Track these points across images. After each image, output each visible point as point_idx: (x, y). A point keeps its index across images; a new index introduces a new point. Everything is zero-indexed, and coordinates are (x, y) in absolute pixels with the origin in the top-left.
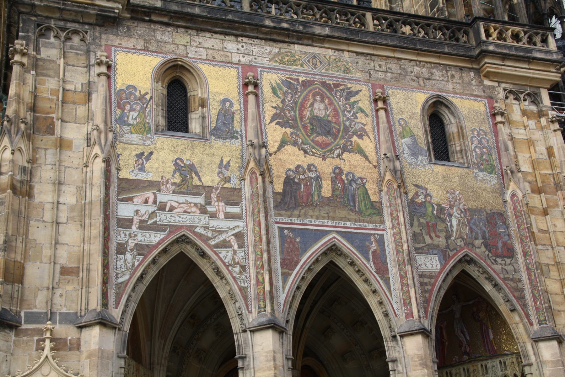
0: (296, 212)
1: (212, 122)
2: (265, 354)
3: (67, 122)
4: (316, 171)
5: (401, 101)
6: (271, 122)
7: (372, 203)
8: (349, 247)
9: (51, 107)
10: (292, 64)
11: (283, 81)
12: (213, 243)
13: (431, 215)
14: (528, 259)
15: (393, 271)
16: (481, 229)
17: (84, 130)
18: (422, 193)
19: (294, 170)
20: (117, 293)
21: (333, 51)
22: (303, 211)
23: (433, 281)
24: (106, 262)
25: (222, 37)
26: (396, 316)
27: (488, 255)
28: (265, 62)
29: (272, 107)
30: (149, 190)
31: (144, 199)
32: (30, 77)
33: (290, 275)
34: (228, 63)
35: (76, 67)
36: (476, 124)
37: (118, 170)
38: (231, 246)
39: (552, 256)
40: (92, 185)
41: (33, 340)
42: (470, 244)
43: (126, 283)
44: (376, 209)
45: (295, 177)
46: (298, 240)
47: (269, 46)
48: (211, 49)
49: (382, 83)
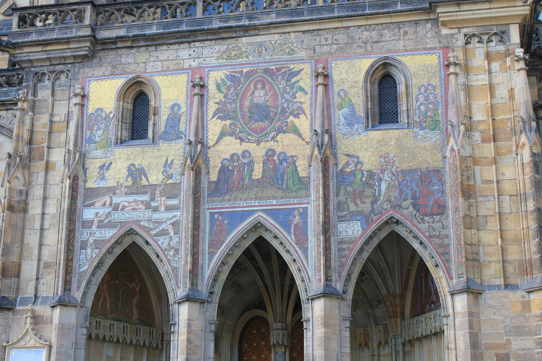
0: (227, 197)
1: (162, 127)
4: (250, 156)
5: (343, 71)
6: (213, 117)
7: (300, 179)
8: (273, 222)
9: (43, 139)
11: (227, 77)
12: (154, 232)
13: (359, 182)
18: (353, 161)
20: (79, 280)
21: (280, 35)
22: (233, 195)
23: (351, 246)
24: (70, 257)
25: (177, 46)
26: (310, 282)
27: (415, 215)
28: (213, 61)
29: (216, 103)
30: (107, 195)
31: (103, 203)
33: (216, 253)
34: (180, 70)
36: (424, 80)
37: (85, 182)
38: (168, 234)
39: (493, 207)
42: (397, 206)
44: (304, 184)
46: (226, 222)
48: (167, 60)
49: (325, 57)
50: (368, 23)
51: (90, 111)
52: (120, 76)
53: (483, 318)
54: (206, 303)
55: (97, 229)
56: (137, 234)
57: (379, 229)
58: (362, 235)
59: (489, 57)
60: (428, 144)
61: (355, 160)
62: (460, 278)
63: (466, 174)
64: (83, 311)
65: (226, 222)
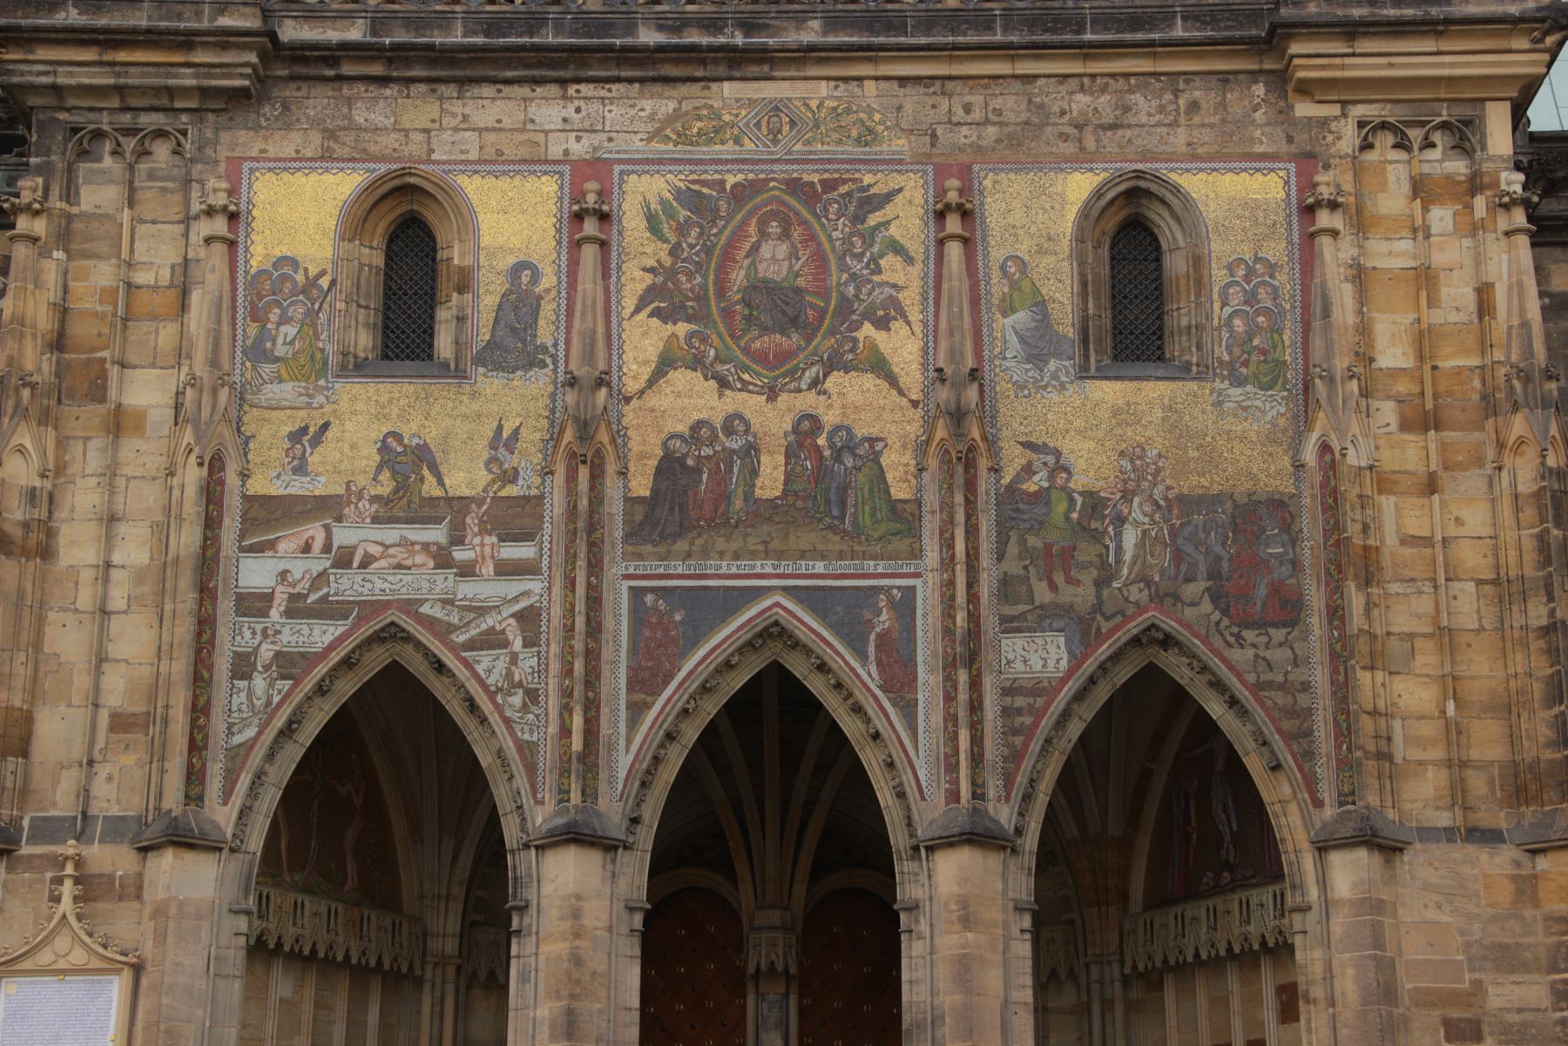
0: (682, 545)
1: (482, 329)
2: (558, 903)
3: (134, 367)
4: (747, 432)
5: (1017, 204)
6: (637, 310)
7: (893, 504)
8: (815, 625)
9: (99, 335)
10: (711, 141)
11: (678, 194)
12: (462, 639)
14: (1336, 628)
15: (928, 683)
16: (1207, 553)
17: (173, 380)
18: (1045, 464)
19: (687, 433)
21: (832, 84)
22: (699, 542)
23: (1040, 702)
25: (525, 91)
26: (923, 798)
27: (1218, 623)
28: (637, 143)
29: (644, 269)
30: (316, 519)
31: (302, 543)
32: (51, 270)
33: (649, 706)
34: (536, 163)
35: (159, 226)
37: (245, 476)
38: (506, 644)
40: (180, 518)
41: (44, 880)
42: (1167, 595)
43: (250, 746)
44: (905, 518)
45: (686, 455)
46: (678, 618)
47: (652, 97)
48: (494, 129)
49: (964, 158)
50: (1089, 71)
51: (254, 263)
52: (351, 165)
53: (1409, 919)
54: (620, 850)
55: (284, 620)
56: (408, 638)
57: (1115, 657)
58: (1070, 673)
59: (1421, 189)
60: (1253, 428)
61: (1051, 459)
62: (1341, 804)
63: (1358, 517)
64: (235, 866)
65: (678, 618)
